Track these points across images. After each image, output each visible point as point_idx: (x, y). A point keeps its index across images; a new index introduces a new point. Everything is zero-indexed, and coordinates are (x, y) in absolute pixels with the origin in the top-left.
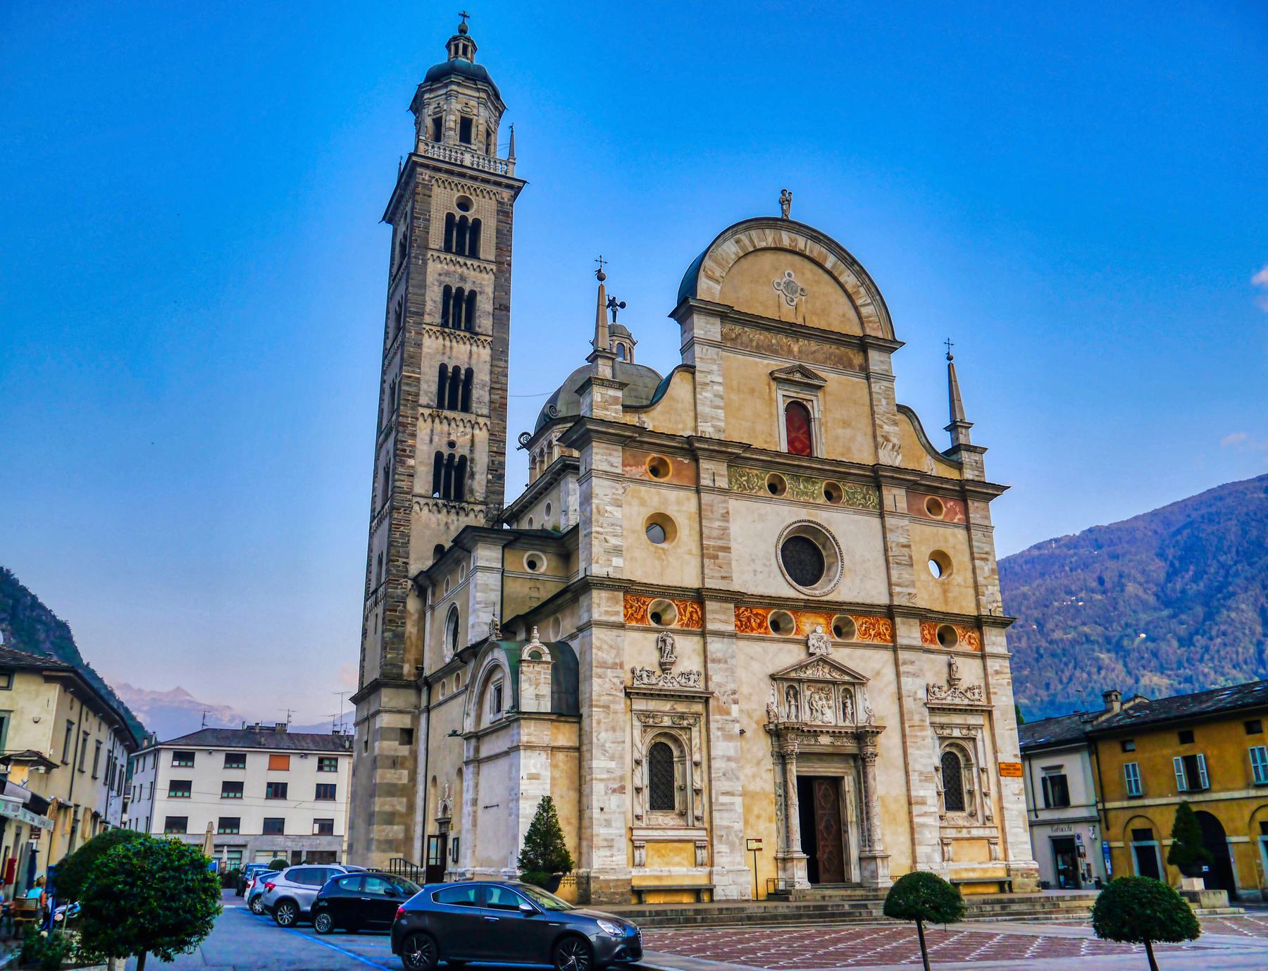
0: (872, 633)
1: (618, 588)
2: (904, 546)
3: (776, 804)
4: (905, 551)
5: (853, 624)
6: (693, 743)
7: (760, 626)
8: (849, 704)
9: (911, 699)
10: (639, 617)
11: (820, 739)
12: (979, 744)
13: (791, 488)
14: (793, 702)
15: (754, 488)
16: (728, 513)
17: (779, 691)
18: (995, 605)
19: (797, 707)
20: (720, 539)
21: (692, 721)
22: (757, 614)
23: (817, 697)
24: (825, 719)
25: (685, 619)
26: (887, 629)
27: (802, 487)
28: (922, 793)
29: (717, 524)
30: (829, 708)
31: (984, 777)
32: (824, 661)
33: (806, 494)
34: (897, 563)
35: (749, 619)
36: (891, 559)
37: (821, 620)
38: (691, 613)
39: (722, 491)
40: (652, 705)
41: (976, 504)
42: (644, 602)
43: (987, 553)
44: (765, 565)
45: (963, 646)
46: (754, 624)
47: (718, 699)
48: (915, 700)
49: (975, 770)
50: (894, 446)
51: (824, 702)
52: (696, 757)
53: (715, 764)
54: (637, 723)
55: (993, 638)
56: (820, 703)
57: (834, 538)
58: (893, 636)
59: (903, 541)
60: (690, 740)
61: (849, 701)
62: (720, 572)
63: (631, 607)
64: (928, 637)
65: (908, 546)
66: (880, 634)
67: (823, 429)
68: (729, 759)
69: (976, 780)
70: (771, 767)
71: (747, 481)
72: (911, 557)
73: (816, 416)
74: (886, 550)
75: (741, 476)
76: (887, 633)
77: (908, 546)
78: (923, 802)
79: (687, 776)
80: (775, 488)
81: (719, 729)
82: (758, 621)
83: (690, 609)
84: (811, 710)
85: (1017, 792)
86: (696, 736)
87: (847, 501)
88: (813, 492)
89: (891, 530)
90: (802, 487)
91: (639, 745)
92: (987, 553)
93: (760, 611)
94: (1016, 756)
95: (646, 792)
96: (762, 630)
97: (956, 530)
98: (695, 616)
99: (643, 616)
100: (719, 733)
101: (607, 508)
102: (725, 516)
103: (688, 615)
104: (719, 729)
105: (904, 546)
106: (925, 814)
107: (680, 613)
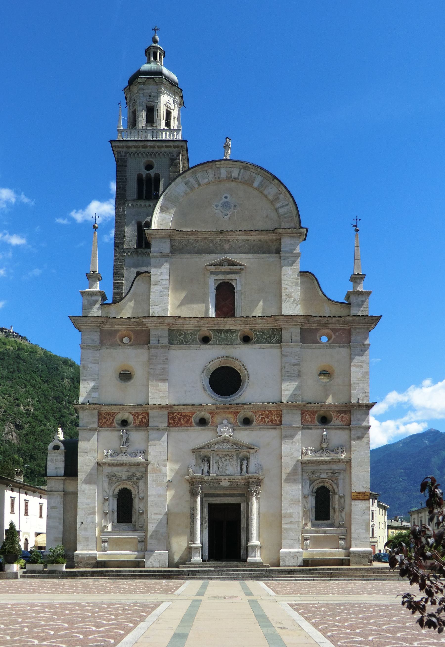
0: (266, 420)
1: (94, 409)
2: (294, 365)
3: (191, 519)
4: (296, 368)
5: (253, 416)
6: (140, 488)
7: (187, 422)
8: (245, 462)
9: (289, 457)
10: (109, 423)
11: (221, 484)
12: (341, 482)
13: (215, 338)
14: (206, 464)
15: (188, 341)
16: (167, 359)
17: (196, 458)
18: (363, 395)
19: (209, 467)
20: (160, 375)
21: (139, 477)
22: (185, 416)
23: (223, 460)
24: (227, 472)
25: (138, 422)
26: (277, 417)
27: (223, 336)
28: (290, 511)
29: (159, 366)
30: (231, 466)
31: (342, 501)
32: (226, 440)
33: (226, 340)
34: (288, 376)
35: (180, 419)
36: (284, 374)
37: (231, 416)
38: (142, 419)
39: (163, 346)
40: (115, 469)
41: (357, 330)
42: (113, 415)
43: (362, 362)
44: (193, 386)
45: (336, 421)
46: (182, 421)
47: (154, 465)
48: (291, 458)
49: (337, 497)
50: (294, 301)
51: (228, 462)
52: (142, 495)
53: (150, 499)
54: (107, 480)
55: (359, 416)
56: (225, 463)
57: (243, 365)
58: (281, 421)
59: (294, 361)
60: (138, 487)
61: (245, 462)
62: (159, 394)
63: (105, 418)
64: (309, 419)
65: (299, 364)
66: (272, 420)
67: (242, 297)
68: (159, 496)
69: (337, 503)
70: (189, 499)
71: (184, 338)
72: (299, 371)
73: (238, 289)
74: (282, 369)
75: (180, 335)
76: (278, 420)
77: (299, 364)
78: (290, 516)
79: (137, 505)
80: (206, 340)
81: (153, 480)
82: (186, 420)
83: (141, 417)
84: (219, 468)
85: (364, 508)
86: (141, 483)
87: (257, 340)
88: (231, 339)
89: (286, 356)
90: (223, 336)
91: (107, 490)
92: (362, 362)
93: (188, 414)
94: (366, 488)
95: (116, 514)
96: (188, 425)
97: (341, 349)
98: (144, 420)
99: (111, 423)
100: (154, 483)
101: (90, 365)
102: (166, 361)
103: (140, 420)
104: (153, 480)
105: (294, 365)
106: (291, 523)
107: (135, 419)
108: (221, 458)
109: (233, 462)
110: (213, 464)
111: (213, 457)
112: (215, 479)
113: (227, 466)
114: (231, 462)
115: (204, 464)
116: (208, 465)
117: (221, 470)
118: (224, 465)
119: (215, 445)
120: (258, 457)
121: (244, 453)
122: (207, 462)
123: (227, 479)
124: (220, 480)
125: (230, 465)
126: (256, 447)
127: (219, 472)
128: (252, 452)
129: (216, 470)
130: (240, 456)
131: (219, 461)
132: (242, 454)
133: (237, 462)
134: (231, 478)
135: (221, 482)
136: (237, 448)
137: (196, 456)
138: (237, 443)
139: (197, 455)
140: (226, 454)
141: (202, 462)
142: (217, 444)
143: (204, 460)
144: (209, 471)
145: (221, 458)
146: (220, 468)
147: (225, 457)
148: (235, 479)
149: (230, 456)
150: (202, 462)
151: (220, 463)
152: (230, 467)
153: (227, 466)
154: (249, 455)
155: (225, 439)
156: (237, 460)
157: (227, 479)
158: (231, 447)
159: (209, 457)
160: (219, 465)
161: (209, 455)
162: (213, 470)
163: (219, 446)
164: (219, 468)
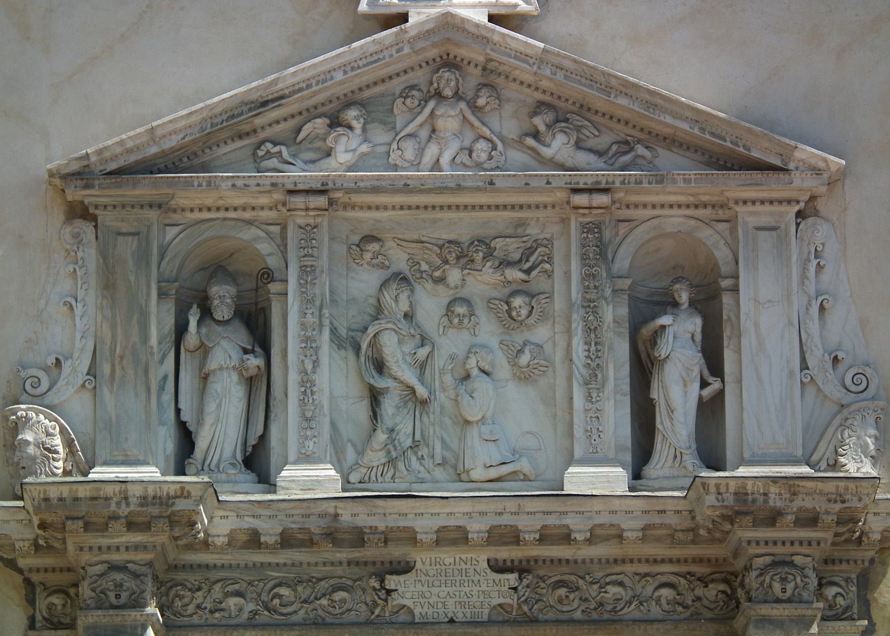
30: (525, 376)
84: (375, 397)
108: (401, 279)
109: (541, 333)
110: (309, 344)
111: (306, 271)
112: (333, 536)
113: (481, 384)
114: (518, 338)
115: (204, 350)
116: (255, 362)
117: (405, 428)
118: (439, 361)
119: (335, 122)
120: (827, 276)
121: (674, 220)
122: (240, 336)
123: (477, 527)
124: (395, 552)
125: (503, 371)
126: (807, 152)
127: (376, 457)
128: (765, 215)
129: (347, 431)
130: (623, 261)
131: (378, 312)
132: (640, 234)
133: (592, 331)
134: (529, 525)
135: (404, 568)
136: (583, 157)
137: (103, 254)
138: (584, 109)
139: (127, 247)
140: (465, 237)
141: (181, 329)
142: (351, 114)
143: (206, 312)
144: (263, 438)
145: (401, 279)
146: (388, 406)
147: (454, 275)
148: (566, 538)
149: (505, 263)
150: (181, 329)
151: (390, 346)
152: (513, 391)
153: (481, 384)
154: (722, 254)
155: (450, 63)
156: (590, 306)
157: (477, 527)
158: (516, 156)
159: (267, 275)
160: (380, 366)
161: (265, 247)
162: (307, 420)
163: (381, 136)
164: (375, 397)
